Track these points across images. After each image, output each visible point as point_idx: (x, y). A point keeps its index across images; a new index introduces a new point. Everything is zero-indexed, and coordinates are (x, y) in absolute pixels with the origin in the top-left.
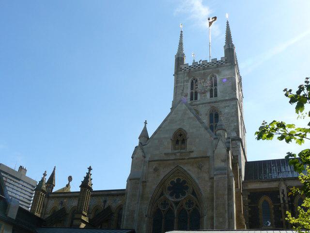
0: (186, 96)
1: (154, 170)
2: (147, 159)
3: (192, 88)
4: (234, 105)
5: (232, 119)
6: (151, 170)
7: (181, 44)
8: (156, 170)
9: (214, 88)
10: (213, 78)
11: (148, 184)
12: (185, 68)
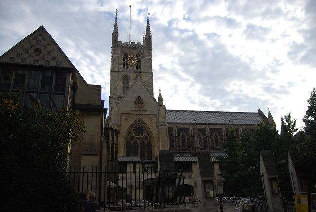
1: (125, 119)
2: (121, 112)
3: (124, 59)
7: (116, 24)
8: (126, 119)
11: (122, 127)
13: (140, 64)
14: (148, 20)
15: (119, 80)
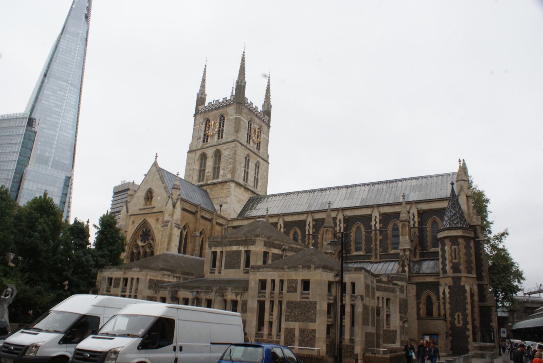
0: (200, 138)
2: (129, 214)
4: (233, 147)
5: (230, 160)
6: (131, 222)
7: (204, 80)
8: (133, 222)
9: (221, 130)
10: (222, 118)
12: (202, 109)
13: (223, 130)
14: (244, 55)
15: (195, 162)
